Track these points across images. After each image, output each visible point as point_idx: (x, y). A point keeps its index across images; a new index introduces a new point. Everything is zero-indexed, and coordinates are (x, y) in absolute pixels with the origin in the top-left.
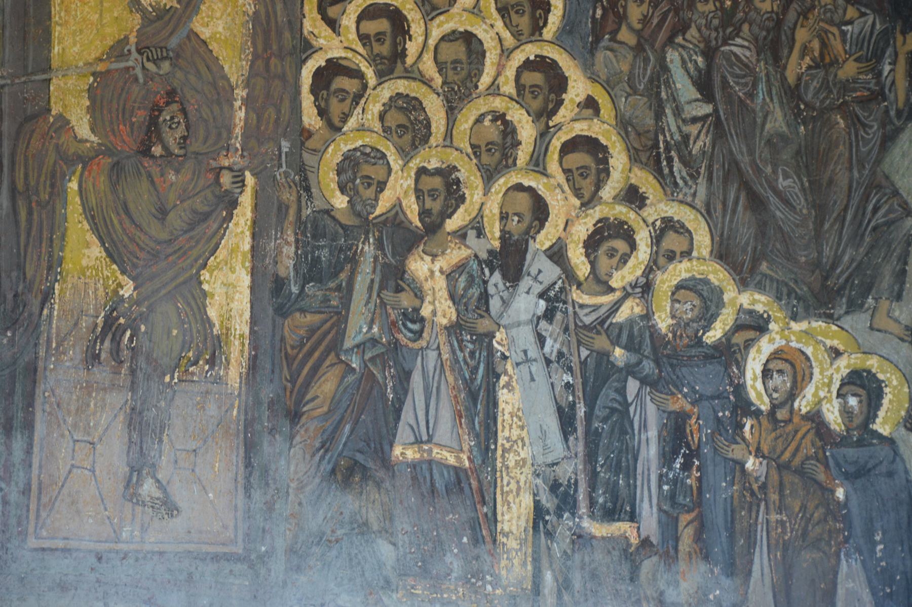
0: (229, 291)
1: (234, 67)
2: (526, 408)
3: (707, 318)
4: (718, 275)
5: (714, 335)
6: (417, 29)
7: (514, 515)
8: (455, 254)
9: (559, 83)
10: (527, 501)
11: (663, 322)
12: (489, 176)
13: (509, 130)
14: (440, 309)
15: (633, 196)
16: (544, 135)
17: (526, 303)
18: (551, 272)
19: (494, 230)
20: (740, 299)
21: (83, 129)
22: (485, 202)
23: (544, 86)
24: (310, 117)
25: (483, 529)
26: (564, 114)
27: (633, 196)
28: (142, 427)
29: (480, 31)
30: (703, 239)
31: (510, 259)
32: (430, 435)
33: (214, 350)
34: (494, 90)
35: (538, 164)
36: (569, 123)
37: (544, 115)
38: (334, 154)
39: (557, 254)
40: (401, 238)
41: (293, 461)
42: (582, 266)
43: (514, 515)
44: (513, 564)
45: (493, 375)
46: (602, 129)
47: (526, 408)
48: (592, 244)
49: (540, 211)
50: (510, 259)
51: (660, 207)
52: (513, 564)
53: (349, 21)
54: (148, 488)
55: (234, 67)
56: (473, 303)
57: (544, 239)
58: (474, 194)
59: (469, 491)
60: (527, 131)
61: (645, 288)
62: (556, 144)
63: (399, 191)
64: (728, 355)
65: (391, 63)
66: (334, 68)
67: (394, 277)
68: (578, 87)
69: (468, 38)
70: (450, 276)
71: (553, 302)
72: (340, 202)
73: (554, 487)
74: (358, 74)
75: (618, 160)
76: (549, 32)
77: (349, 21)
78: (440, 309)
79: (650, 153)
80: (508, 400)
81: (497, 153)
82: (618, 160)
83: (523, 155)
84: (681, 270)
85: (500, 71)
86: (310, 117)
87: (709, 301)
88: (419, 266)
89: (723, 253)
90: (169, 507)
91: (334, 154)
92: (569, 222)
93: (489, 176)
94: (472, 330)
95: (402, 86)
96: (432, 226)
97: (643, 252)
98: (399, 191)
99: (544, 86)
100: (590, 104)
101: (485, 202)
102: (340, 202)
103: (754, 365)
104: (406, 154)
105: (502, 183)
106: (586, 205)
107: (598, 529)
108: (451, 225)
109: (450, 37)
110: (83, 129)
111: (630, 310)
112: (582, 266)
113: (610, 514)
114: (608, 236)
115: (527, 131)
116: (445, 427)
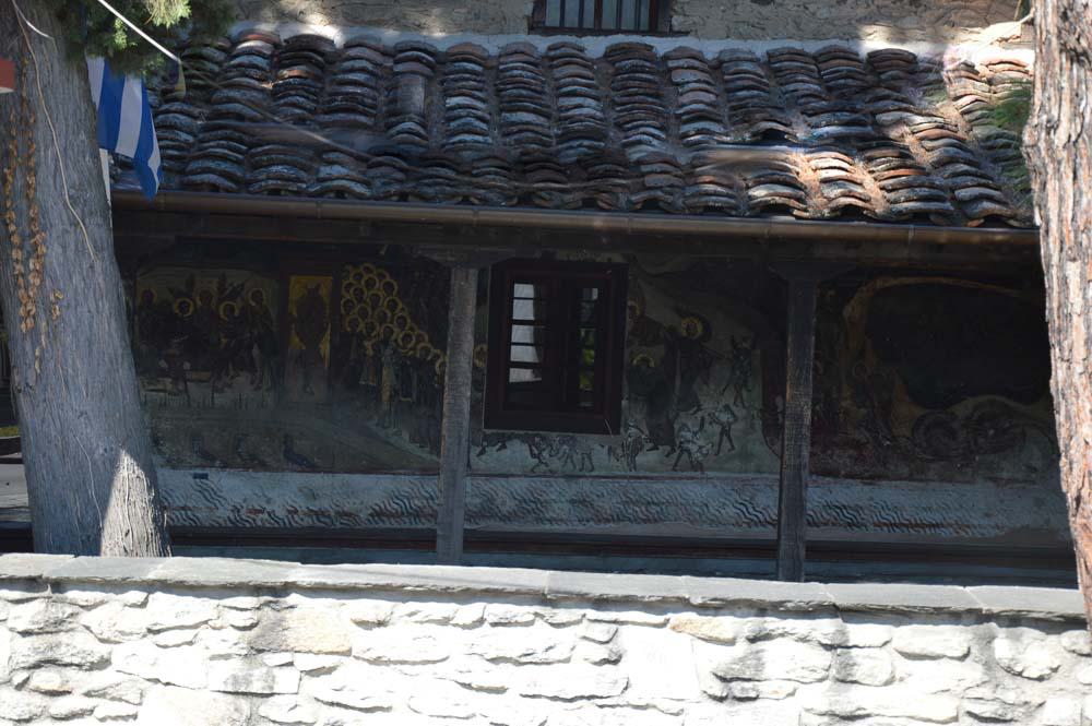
0: (325, 348)
1: (326, 300)
2: (388, 377)
3: (427, 355)
4: (429, 345)
5: (429, 358)
6: (366, 293)
7: (386, 396)
8: (374, 341)
9: (396, 305)
10: (388, 393)
11: (418, 355)
12: (381, 324)
13: (385, 314)
15: (412, 329)
16: (393, 316)
17: (389, 352)
18: (394, 345)
19: (382, 336)
20: (434, 351)
21: (295, 314)
22: (380, 329)
23: (393, 306)
24: (343, 311)
25: (379, 400)
26: (397, 311)
27: (412, 329)
29: (380, 293)
30: (427, 338)
33: (322, 359)
34: (382, 306)
35: (392, 322)
36: (398, 313)
37: (393, 311)
38: (348, 319)
39: (396, 341)
42: (401, 343)
43: (386, 396)
44: (385, 407)
45: (382, 366)
46: (405, 314)
47: (388, 377)
48: (403, 339)
49: (392, 332)
50: (386, 342)
51: (418, 331)
52: (385, 407)
53: (351, 292)
54: (308, 389)
55: (326, 300)
57: (394, 337)
58: (378, 328)
59: (376, 391)
60: (389, 314)
61: (414, 349)
62: (395, 318)
63: (361, 327)
64: (432, 362)
66: (348, 301)
67: (360, 345)
68: (400, 306)
69: (377, 295)
70: (372, 345)
71: (395, 351)
72: (349, 329)
73: (394, 390)
74: (352, 302)
75: (409, 321)
76: (395, 293)
77: (351, 292)
78: (370, 352)
79: (414, 319)
80: (385, 372)
81: (383, 319)
82: (409, 321)
83: (389, 320)
84: (422, 345)
86: (343, 311)
87: (428, 351)
88: (366, 343)
89: (431, 341)
90: (312, 393)
91: (348, 319)
92: (398, 334)
93: (381, 324)
95: (362, 305)
96: (369, 334)
97: (414, 341)
98: (361, 327)
99: (393, 306)
100: (403, 309)
101: (380, 329)
102: (349, 329)
103: (437, 365)
104: (363, 320)
105: (384, 325)
106: (403, 330)
107: (403, 399)
108: (374, 334)
109: (373, 295)
110: (295, 314)
111: (411, 353)
112: (401, 343)
113: (405, 397)
114: (407, 337)
115: (389, 314)
116: (371, 378)
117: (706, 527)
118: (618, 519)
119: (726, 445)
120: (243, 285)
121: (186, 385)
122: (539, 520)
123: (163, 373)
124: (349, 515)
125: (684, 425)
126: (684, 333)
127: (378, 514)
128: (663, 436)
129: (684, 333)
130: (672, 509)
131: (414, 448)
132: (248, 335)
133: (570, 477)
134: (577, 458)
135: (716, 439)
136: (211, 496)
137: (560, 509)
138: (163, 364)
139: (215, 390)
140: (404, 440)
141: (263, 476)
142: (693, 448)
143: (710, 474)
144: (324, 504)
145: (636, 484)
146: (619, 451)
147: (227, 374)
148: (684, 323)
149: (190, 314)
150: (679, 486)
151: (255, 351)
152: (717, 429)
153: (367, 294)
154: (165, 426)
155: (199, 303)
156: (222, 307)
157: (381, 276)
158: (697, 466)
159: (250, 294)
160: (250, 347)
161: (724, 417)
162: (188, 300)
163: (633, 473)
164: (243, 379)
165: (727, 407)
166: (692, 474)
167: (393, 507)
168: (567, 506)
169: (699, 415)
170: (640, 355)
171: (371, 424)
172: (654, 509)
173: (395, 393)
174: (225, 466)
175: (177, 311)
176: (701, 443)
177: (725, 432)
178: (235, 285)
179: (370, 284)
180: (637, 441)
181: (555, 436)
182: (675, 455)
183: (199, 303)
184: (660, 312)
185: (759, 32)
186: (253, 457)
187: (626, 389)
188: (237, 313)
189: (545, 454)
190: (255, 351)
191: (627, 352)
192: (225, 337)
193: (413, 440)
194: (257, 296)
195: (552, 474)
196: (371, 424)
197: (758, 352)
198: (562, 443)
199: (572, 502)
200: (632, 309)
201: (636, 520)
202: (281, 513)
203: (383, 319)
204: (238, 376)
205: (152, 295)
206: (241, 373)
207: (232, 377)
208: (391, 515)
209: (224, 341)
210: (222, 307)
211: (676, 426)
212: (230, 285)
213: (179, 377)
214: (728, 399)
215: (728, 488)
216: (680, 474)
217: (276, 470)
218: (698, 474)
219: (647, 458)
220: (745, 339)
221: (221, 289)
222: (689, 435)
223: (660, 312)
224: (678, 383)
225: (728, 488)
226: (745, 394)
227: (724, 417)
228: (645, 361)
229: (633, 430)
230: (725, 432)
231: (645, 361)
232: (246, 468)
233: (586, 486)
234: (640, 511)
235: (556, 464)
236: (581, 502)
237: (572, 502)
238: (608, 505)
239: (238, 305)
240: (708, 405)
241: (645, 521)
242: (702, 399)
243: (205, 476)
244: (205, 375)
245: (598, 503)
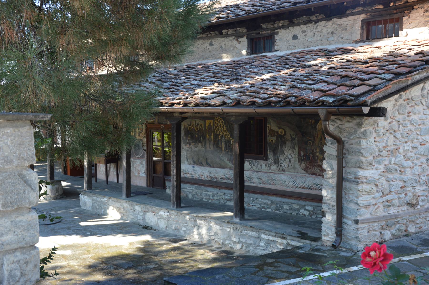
0: (212, 138)
7: (223, 149)
14: (220, 139)
22: (221, 133)
23: (223, 127)
25: (222, 150)
28: (210, 144)
31: (222, 136)
32: (220, 146)
33: (212, 140)
40: (219, 135)
41: (215, 146)
43: (223, 149)
44: (223, 152)
50: (222, 136)
52: (223, 152)
56: (221, 138)
59: (221, 148)
64: (230, 141)
65: (218, 126)
67: (218, 137)
78: (220, 139)
81: (222, 130)
85: (222, 126)
92: (224, 134)
94: (221, 140)
99: (223, 127)
114: (226, 135)
117: (285, 187)
118: (267, 183)
119: (290, 165)
122: (251, 182)
123: (188, 143)
124: (217, 178)
125: (281, 159)
126: (280, 133)
127: (222, 178)
128: (277, 162)
129: (280, 133)
130: (278, 182)
131: (228, 162)
133: (257, 172)
134: (259, 166)
135: (288, 163)
136: (195, 171)
137: (255, 180)
138: (187, 141)
139: (196, 147)
140: (226, 160)
141: (203, 167)
142: (283, 165)
143: (287, 173)
144: (212, 175)
145: (271, 174)
146: (267, 165)
148: (280, 130)
150: (280, 175)
151: (201, 138)
152: (288, 160)
153: (219, 124)
154: (188, 155)
157: (221, 120)
158: (284, 170)
161: (290, 157)
163: (270, 171)
164: (200, 145)
165: (290, 154)
166: (282, 172)
167: (224, 177)
168: (256, 179)
169: (284, 156)
170: (271, 139)
171: (221, 156)
172: (274, 181)
173: (225, 149)
174: (197, 165)
176: (285, 164)
177: (290, 161)
179: (219, 122)
180: (271, 163)
181: (254, 160)
182: (279, 167)
184: (274, 128)
185: (294, 47)
186: (201, 163)
187: (268, 149)
189: (252, 165)
190: (201, 138)
191: (268, 138)
193: (228, 161)
194: (201, 125)
195: (254, 171)
196: (221, 156)
197: (297, 139)
198: (256, 162)
199: (258, 178)
200: (268, 127)
201: (270, 184)
202: (206, 177)
203: (222, 130)
208: (224, 179)
211: (279, 159)
213: (190, 144)
214: (290, 152)
215: (290, 177)
216: (280, 172)
217: (205, 166)
218: (284, 172)
219: (274, 167)
220: (293, 135)
221: (196, 124)
222: (282, 161)
223: (274, 128)
224: (279, 147)
225: (290, 177)
226: (294, 150)
227: (290, 157)
228: (272, 141)
229: (270, 160)
230: (290, 161)
231: (272, 141)
232: (200, 165)
233: (260, 174)
234: (271, 182)
235: (255, 168)
236: (259, 178)
237: (258, 178)
238: (265, 179)
239: (198, 127)
240: (286, 153)
241: (273, 185)
242: (285, 152)
243: (194, 167)
244: (194, 144)
245: (263, 179)
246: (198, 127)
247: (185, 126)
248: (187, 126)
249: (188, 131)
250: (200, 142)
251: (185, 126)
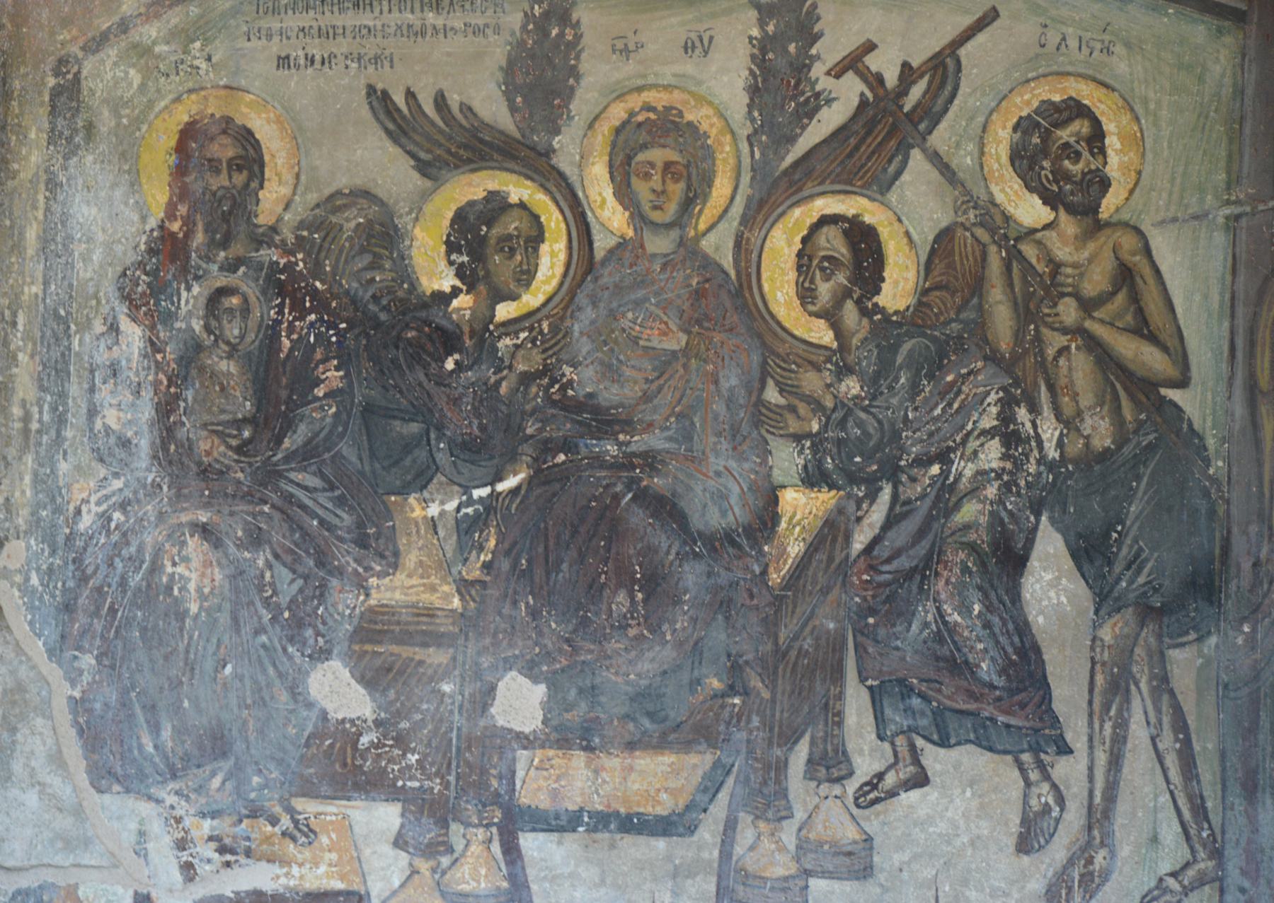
120: (943, 69)
121: (511, 851)
123: (346, 766)
132: (992, 455)
138: (338, 691)
147: (830, 764)
149: (532, 299)
151: (1051, 587)
155: (611, 218)
156: (782, 244)
159: (1002, 139)
160: (1007, 558)
162: (519, 190)
175: (437, 276)
178: (886, 64)
183: (611, 218)
188: (897, 291)
190: (1051, 587)
192: (813, 478)
194: (1057, 151)
204: (920, 780)
205: (250, 159)
206: (935, 758)
207: (873, 793)
209: (801, 506)
210: (782, 244)
212: (853, 63)
239: (908, 215)
244: (657, 778)
246: (908, 215)
247: (218, 164)
248: (384, 166)
249: (403, 337)
250: (1008, 704)
251: (218, 164)
